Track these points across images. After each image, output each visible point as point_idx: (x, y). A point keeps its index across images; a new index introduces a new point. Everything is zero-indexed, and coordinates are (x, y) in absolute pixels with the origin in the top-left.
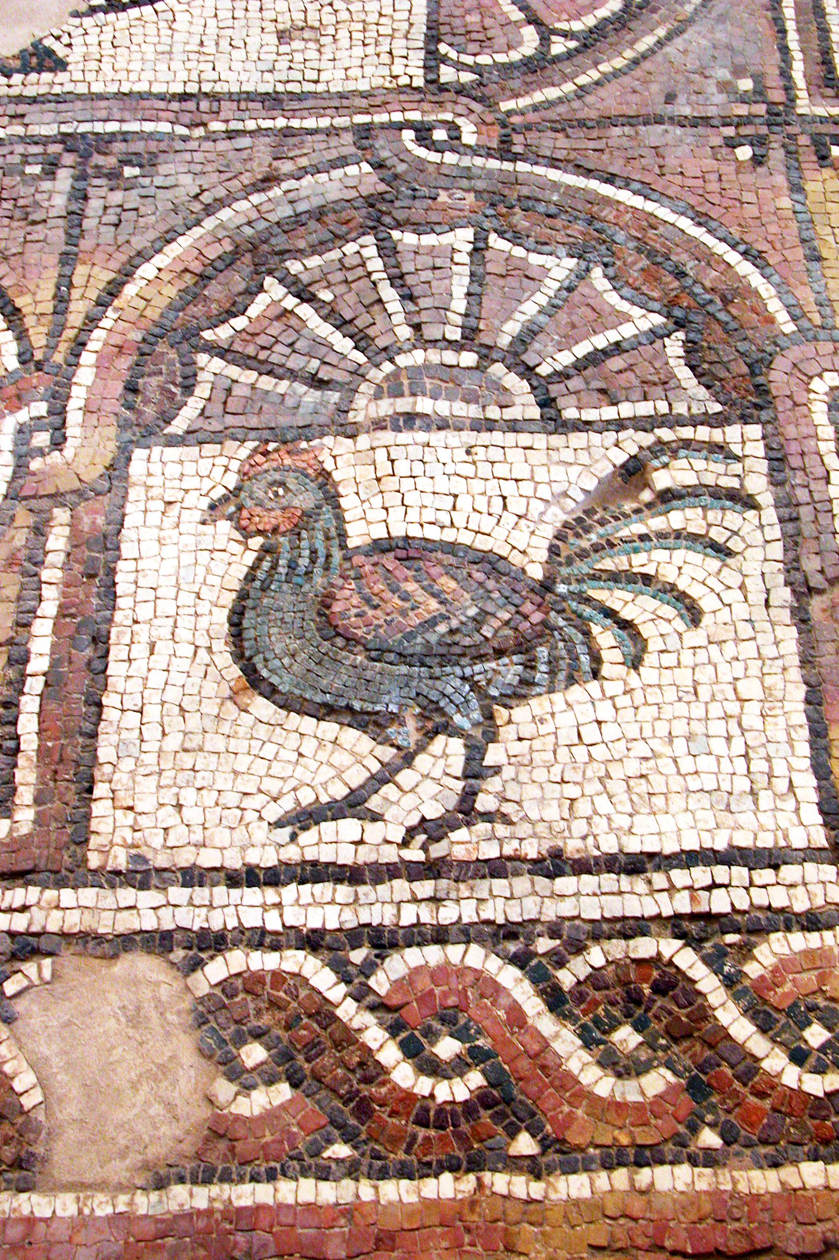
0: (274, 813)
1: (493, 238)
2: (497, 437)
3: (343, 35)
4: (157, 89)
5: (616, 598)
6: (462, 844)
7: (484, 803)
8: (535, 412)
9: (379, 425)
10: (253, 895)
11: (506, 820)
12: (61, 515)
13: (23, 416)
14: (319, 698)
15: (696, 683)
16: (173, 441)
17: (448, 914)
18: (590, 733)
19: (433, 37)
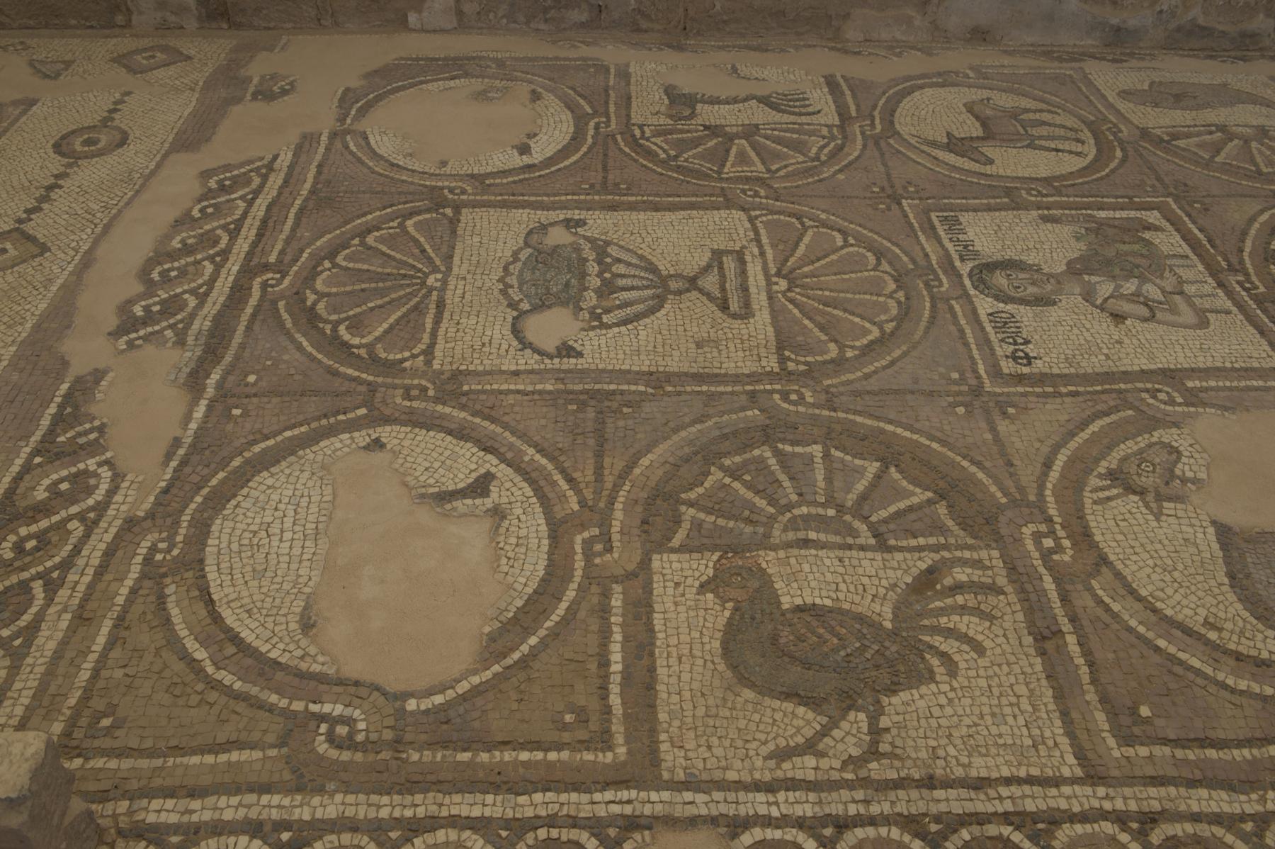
0: (765, 751)
1: (833, 450)
2: (854, 553)
3: (731, 345)
4: (635, 368)
5: (937, 641)
6: (875, 769)
7: (884, 747)
8: (872, 541)
9: (788, 545)
10: (761, 797)
11: (896, 756)
12: (617, 588)
13: (586, 535)
14: (780, 689)
15: (990, 686)
16: (673, 551)
17: (875, 809)
18: (936, 711)
19: (780, 348)
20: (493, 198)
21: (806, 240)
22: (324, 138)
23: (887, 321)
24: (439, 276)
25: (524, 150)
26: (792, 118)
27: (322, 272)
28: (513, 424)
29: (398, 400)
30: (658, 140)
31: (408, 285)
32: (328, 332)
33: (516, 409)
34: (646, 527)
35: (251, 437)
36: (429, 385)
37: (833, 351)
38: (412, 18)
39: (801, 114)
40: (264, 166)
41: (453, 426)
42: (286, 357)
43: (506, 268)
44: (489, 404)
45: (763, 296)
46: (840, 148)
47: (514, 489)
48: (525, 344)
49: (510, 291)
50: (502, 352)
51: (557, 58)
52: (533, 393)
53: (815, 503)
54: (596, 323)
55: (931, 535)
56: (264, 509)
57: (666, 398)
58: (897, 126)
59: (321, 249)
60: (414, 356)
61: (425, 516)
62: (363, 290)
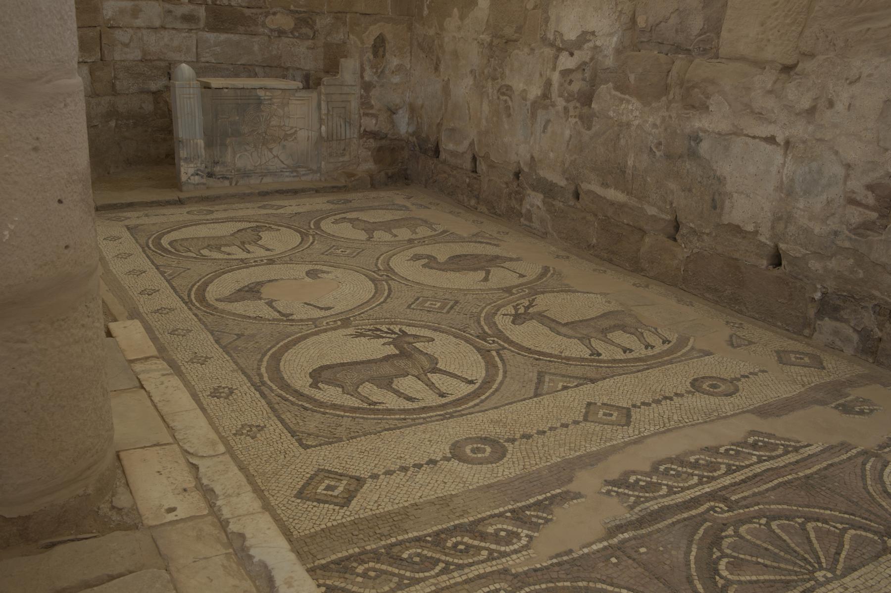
24: (829, 575)
31: (801, 567)
32: (714, 556)
35: (604, 578)
42: (673, 552)
59: (770, 510)
62: (766, 549)
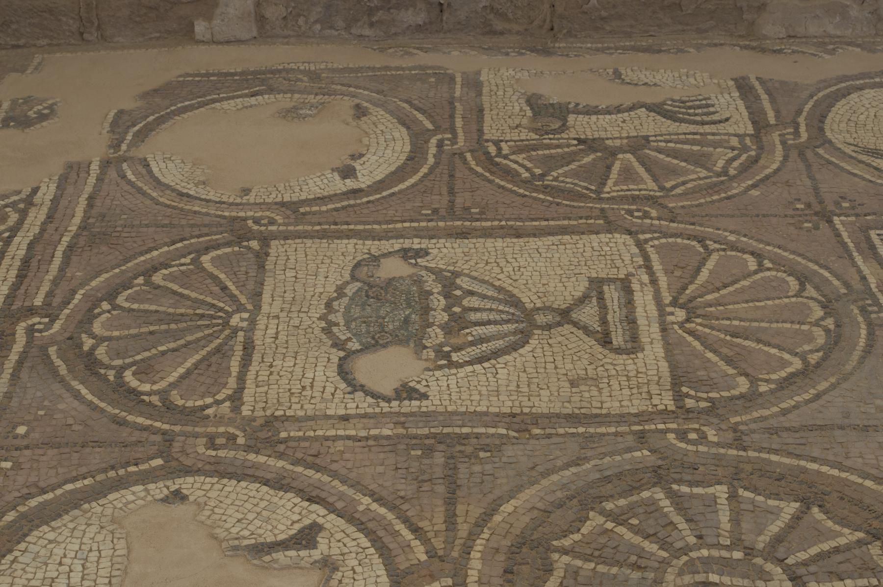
1: (741, 491)
3: (614, 383)
4: (492, 410)
19: (676, 384)
20: (310, 228)
21: (710, 264)
22: (95, 167)
23: (811, 352)
24: (246, 315)
25: (348, 172)
26: (692, 128)
27: (100, 314)
28: (343, 472)
29: (201, 450)
30: (520, 158)
31: (207, 326)
32: (111, 378)
33: (347, 456)
34: (510, 576)
35: (25, 491)
36: (238, 433)
37: (743, 385)
38: (200, 28)
39: (703, 123)
40: (21, 200)
41: (269, 476)
42: (61, 406)
43: (328, 305)
44: (313, 452)
45: (655, 328)
46: (756, 160)
47: (346, 540)
48: (354, 387)
49: (335, 329)
50: (328, 395)
51: (387, 68)
52: (367, 438)
53: (718, 546)
54: (444, 362)
55: (861, 576)
56: (46, 564)
57: (532, 442)
58: (828, 134)
59: (97, 289)
60: (218, 403)
61: (239, 569)
62: (151, 333)
